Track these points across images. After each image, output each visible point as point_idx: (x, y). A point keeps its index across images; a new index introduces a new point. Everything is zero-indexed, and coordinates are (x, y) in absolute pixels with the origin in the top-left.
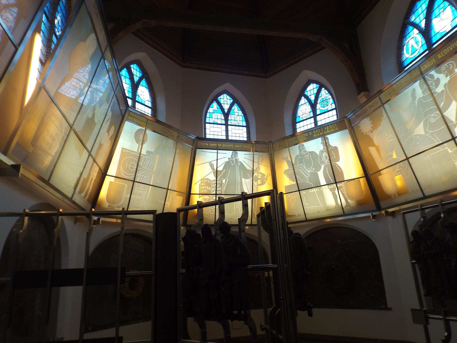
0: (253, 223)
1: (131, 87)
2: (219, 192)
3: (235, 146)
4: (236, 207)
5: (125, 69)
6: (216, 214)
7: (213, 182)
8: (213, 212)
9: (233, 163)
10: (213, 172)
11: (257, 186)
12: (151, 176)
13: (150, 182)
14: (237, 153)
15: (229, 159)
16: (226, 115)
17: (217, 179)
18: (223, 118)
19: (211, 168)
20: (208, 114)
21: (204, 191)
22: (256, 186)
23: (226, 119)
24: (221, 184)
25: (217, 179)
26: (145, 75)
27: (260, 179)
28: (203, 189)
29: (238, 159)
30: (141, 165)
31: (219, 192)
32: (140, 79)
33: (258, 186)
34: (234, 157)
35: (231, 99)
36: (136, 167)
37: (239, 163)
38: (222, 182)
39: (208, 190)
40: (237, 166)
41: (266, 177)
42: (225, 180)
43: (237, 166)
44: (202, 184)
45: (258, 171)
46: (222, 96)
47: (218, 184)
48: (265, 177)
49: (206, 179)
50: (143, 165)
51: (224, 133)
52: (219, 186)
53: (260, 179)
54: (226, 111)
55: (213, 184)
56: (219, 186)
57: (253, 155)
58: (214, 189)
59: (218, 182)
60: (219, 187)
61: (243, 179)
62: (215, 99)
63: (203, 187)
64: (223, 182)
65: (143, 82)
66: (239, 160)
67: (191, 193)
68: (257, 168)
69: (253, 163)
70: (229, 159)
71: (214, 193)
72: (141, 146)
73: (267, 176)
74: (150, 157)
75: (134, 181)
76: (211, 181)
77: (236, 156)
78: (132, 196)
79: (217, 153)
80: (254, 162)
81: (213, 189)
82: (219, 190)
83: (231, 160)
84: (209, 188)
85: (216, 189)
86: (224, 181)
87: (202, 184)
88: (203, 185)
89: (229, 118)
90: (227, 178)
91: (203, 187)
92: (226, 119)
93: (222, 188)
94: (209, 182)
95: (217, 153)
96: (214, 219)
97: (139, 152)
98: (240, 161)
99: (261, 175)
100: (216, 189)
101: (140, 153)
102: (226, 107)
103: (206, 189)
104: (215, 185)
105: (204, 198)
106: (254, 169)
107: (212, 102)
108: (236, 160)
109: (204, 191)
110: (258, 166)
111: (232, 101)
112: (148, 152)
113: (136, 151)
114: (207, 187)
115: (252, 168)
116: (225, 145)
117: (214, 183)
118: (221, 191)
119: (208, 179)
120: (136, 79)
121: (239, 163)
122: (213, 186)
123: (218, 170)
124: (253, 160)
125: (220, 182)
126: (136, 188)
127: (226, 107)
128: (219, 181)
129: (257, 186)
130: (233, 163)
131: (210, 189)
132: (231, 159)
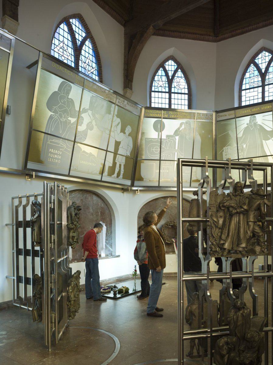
1: (167, 83)
5: (161, 69)
12: (175, 153)
13: (174, 158)
14: (255, 117)
15: (247, 124)
16: (263, 76)
18: (260, 79)
20: (244, 80)
23: (263, 80)
24: (243, 149)
26: (180, 66)
29: (257, 122)
30: (164, 147)
32: (176, 72)
35: (270, 54)
36: (159, 150)
38: (243, 147)
42: (245, 145)
46: (260, 56)
50: (165, 147)
51: (260, 96)
54: (263, 71)
61: (264, 141)
62: (252, 61)
64: (244, 147)
65: (180, 73)
66: (258, 123)
70: (247, 124)
72: (160, 133)
74: (171, 139)
75: (160, 160)
78: (161, 171)
86: (245, 146)
89: (267, 77)
92: (263, 80)
95: (236, 121)
97: (160, 138)
101: (161, 139)
102: (263, 67)
107: (248, 66)
108: (255, 124)
111: (270, 57)
112: (167, 136)
113: (157, 138)
120: (170, 74)
126: (163, 165)
127: (263, 67)
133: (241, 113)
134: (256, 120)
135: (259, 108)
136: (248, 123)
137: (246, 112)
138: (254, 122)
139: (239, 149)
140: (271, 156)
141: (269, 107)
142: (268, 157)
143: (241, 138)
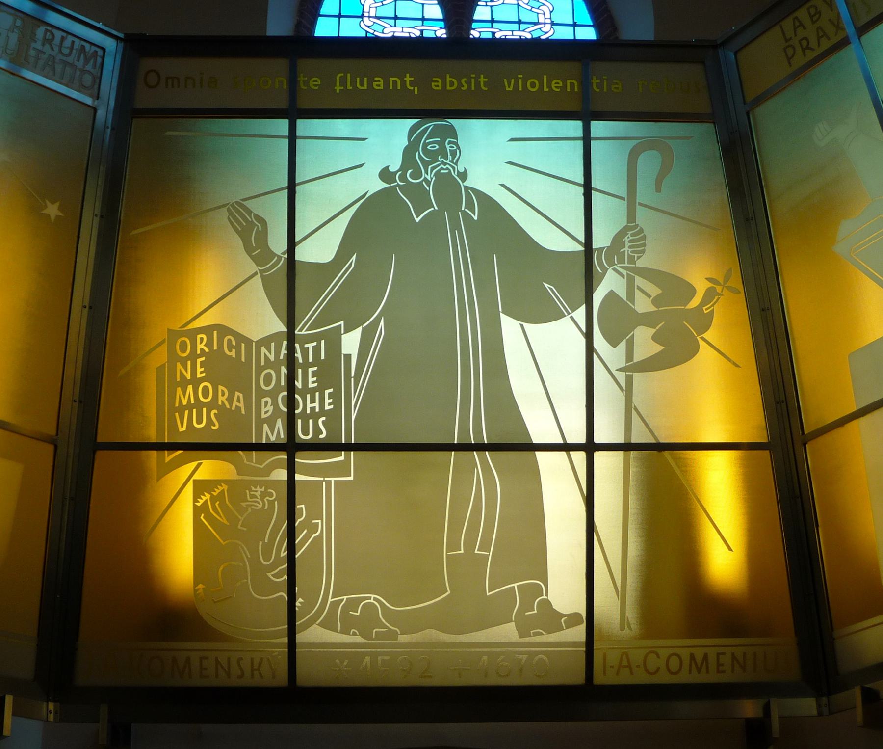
0: (599, 679)
2: (317, 431)
3: (437, 85)
4: (454, 544)
6: (299, 602)
7: (263, 350)
8: (276, 587)
9: (421, 202)
10: (259, 276)
11: (629, 380)
17: (291, 324)
19: (248, 249)
21: (199, 421)
22: (621, 377)
25: (291, 324)
27: (647, 320)
28: (190, 407)
29: (464, 176)
31: (317, 431)
33: (637, 376)
34: (426, 164)
37: (470, 204)
39: (224, 414)
40: (455, 226)
41: (704, 302)
42: (357, 334)
43: (455, 226)
44: (179, 366)
45: (632, 260)
47: (306, 365)
48: (695, 303)
49: (208, 330)
52: (311, 386)
53: (647, 320)
55: (265, 368)
56: (311, 380)
57: (587, 139)
58: (275, 403)
59: (305, 352)
60: (312, 391)
61: (509, 326)
63: (190, 388)
64: (345, 351)
66: (466, 184)
67: (101, 439)
68: (618, 240)
69: (581, 200)
70: (385, 174)
71: (273, 439)
73: (709, 295)
76: (248, 342)
77: (442, 152)
79: (293, 138)
80: (595, 195)
81: (267, 410)
82: (315, 416)
83: (408, 189)
84: (230, 400)
85: (291, 403)
86: (351, 343)
87: (179, 366)
88: (188, 377)
90: (377, 322)
91: (190, 388)
93: (336, 396)
94: (233, 354)
95: (293, 138)
96: (286, 640)
98: (474, 190)
99: (654, 291)
100: (291, 403)
103: (210, 406)
104: (284, 370)
105: (196, 477)
106: (595, 245)
109: (199, 421)
110: (631, 215)
114: (221, 388)
115: (582, 238)
116: (353, 83)
117: (272, 358)
118: (333, 418)
119: (223, 330)
121: (470, 204)
122: (267, 384)
123: (298, 257)
124: (581, 180)
125: (317, 350)
128: (310, 346)
129: (629, 380)
130: (421, 202)
131: (242, 405)
132: (403, 178)
133: (338, 88)
134: (454, 153)
135: (482, 79)
136: (392, 169)
137: (379, 84)
138: (443, 166)
139: (298, 355)
140: (563, 454)
141: (557, 85)
142: (539, 455)
143: (326, 271)
